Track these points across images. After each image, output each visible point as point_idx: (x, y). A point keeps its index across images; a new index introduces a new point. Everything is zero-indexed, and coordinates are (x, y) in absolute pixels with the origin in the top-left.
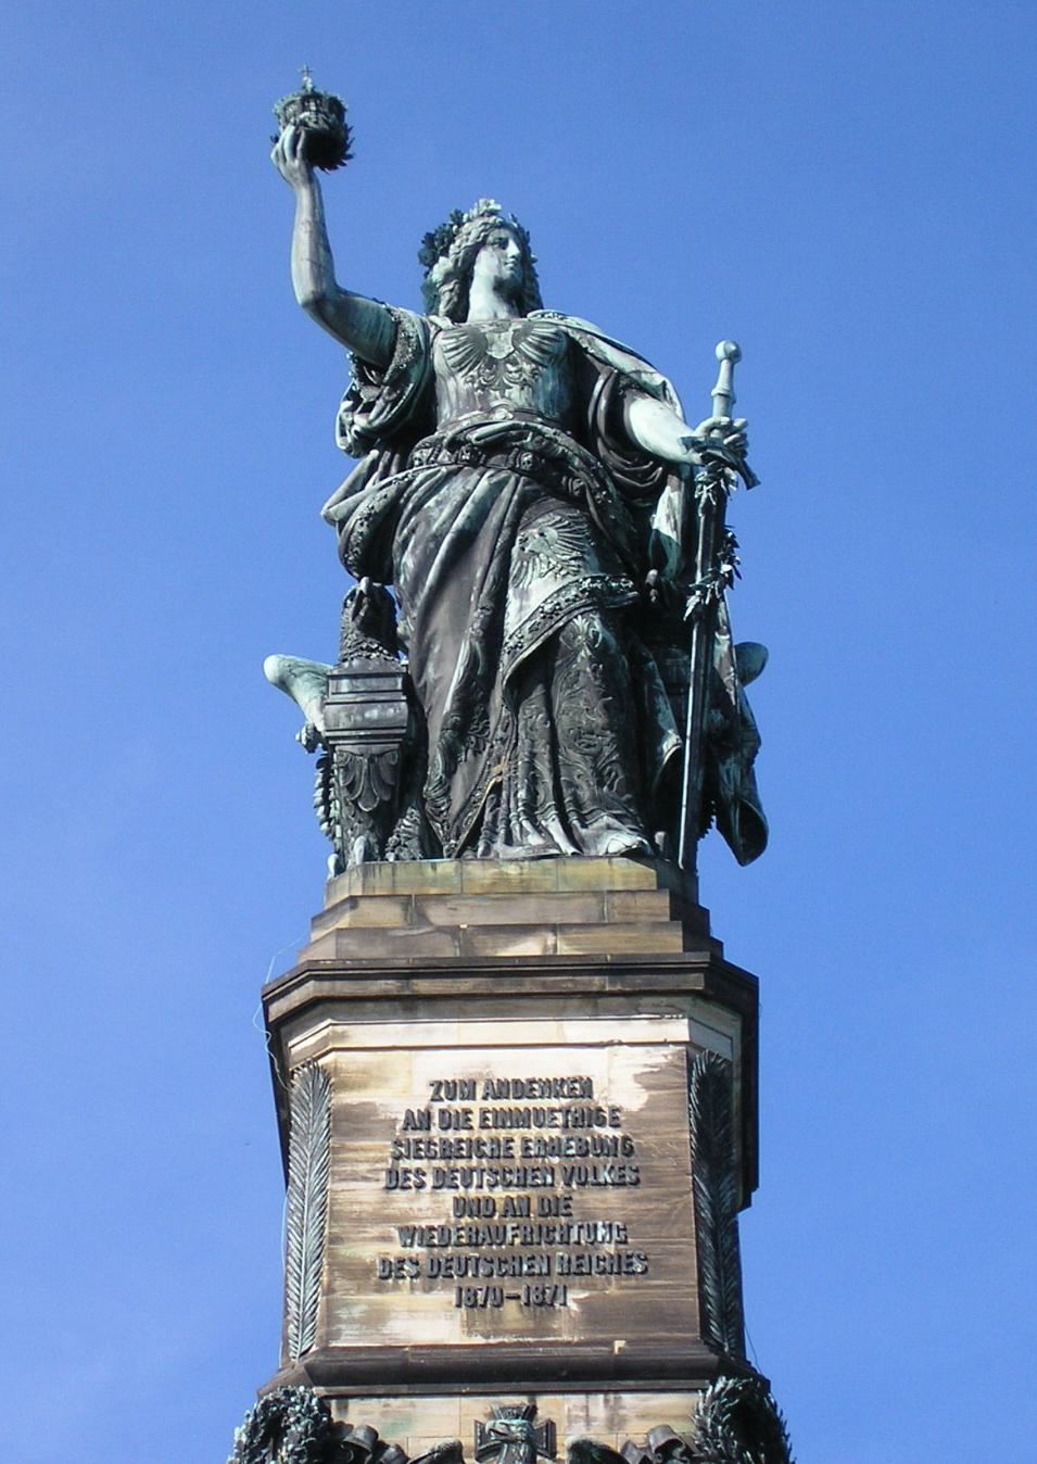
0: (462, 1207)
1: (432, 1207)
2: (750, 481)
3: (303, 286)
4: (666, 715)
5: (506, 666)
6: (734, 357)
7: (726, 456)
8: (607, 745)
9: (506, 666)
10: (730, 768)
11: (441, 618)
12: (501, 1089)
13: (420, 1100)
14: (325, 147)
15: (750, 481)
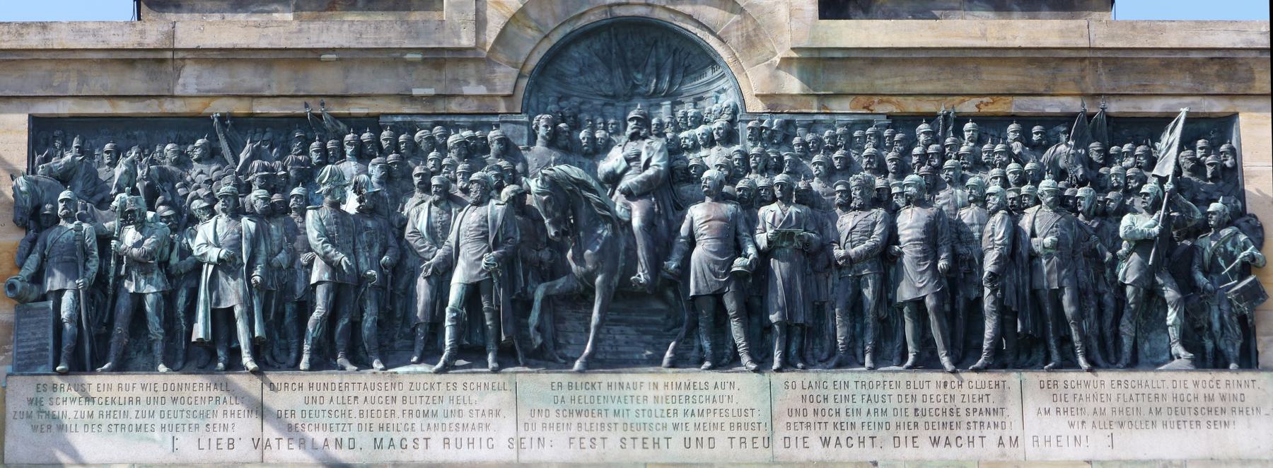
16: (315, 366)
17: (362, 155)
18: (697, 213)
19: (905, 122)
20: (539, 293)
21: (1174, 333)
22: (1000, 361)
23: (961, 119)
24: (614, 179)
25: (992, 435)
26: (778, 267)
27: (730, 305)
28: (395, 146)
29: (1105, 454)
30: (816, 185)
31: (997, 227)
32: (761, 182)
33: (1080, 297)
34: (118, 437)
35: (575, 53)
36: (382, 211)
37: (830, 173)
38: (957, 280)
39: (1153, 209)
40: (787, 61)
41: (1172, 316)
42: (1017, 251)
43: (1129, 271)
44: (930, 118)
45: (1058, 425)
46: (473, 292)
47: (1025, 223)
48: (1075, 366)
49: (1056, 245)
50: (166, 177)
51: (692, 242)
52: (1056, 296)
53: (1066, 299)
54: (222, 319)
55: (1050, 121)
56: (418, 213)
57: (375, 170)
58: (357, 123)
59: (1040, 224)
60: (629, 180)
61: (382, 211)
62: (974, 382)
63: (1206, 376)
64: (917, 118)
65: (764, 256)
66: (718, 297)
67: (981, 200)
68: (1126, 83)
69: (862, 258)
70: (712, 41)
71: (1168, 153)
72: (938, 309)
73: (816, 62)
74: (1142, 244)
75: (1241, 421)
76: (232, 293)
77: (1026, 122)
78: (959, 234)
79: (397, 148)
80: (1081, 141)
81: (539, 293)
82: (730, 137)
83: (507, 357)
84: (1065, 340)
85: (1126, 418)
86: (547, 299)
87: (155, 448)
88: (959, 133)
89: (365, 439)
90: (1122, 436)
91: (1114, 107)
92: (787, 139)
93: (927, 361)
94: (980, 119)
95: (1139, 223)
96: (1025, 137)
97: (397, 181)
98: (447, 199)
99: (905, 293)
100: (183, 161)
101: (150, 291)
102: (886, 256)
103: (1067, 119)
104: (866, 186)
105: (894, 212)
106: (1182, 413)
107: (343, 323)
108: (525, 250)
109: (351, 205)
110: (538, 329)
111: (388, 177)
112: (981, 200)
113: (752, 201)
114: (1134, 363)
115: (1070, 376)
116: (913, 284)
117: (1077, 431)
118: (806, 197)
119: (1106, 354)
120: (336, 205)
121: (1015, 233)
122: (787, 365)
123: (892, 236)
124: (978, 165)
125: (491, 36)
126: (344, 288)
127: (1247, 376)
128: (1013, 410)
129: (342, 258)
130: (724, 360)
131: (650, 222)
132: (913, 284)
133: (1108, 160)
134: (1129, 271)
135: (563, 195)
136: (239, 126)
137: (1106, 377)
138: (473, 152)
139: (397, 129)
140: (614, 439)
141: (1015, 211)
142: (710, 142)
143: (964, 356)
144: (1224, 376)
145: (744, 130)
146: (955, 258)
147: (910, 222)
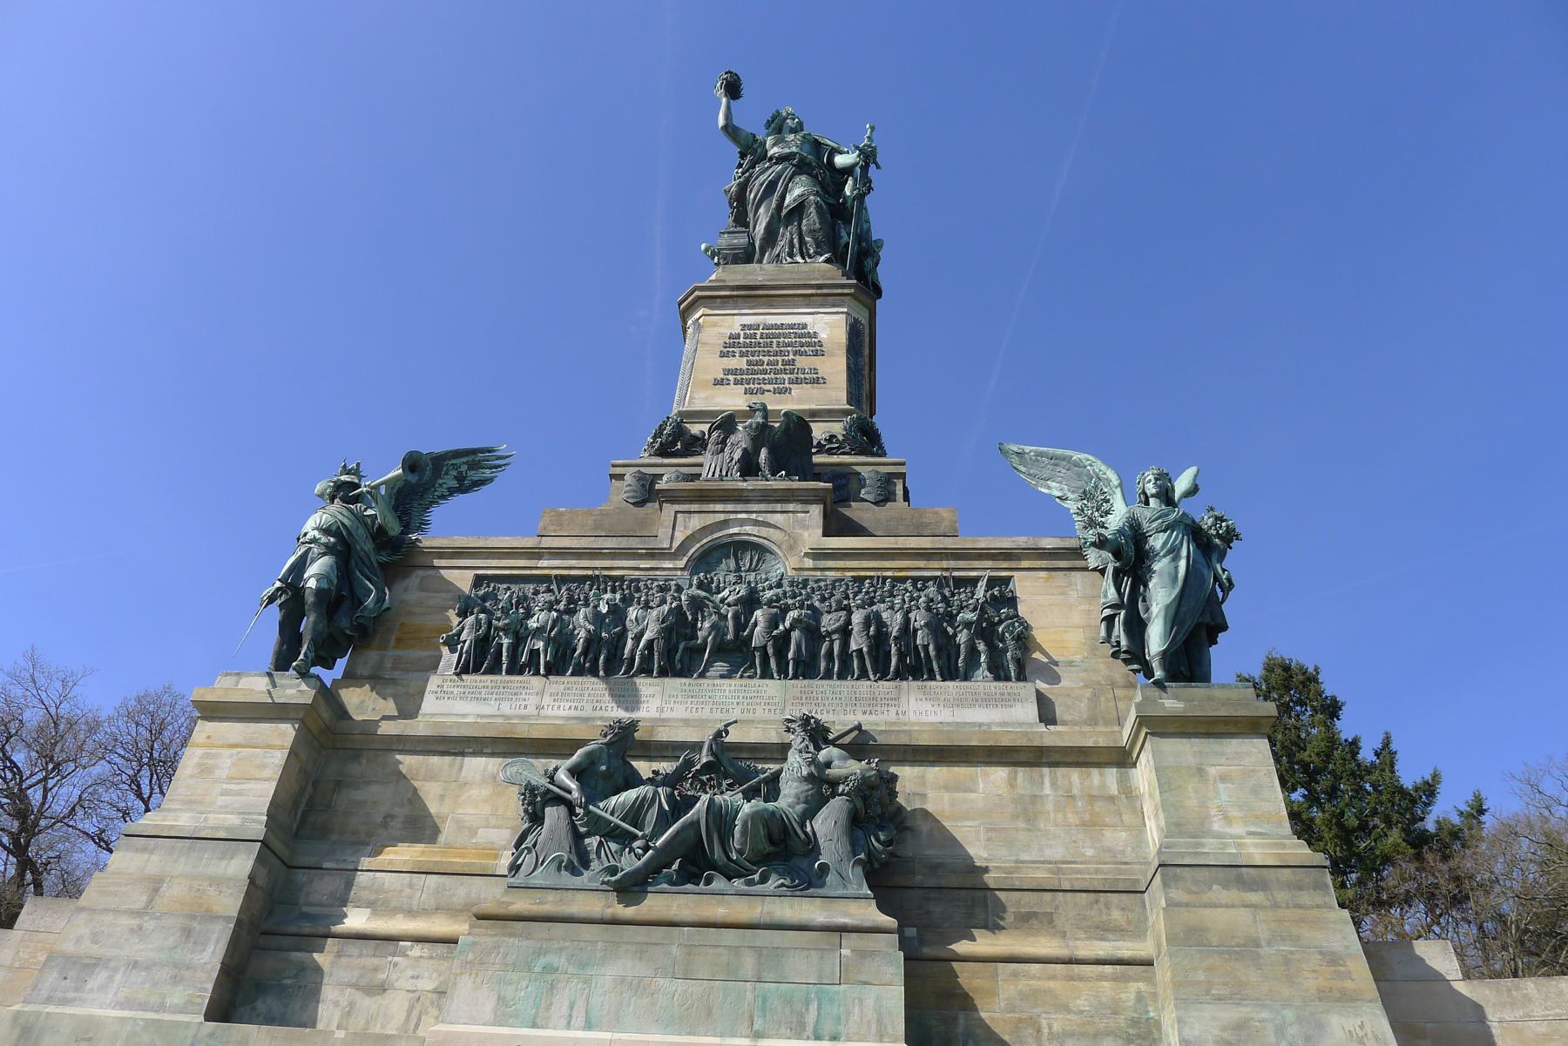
0: (749, 363)
1: (739, 363)
2: (878, 167)
3: (721, 121)
4: (843, 233)
5: (784, 212)
6: (873, 128)
7: (868, 156)
8: (820, 235)
9: (784, 212)
10: (869, 263)
11: (762, 210)
12: (767, 327)
13: (737, 330)
14: (733, 89)
15: (878, 167)
16: (573, 674)
17: (614, 591)
18: (758, 613)
19: (859, 580)
20: (681, 646)
21: (984, 665)
22: (900, 675)
23: (885, 579)
24: (723, 600)
25: (893, 710)
26: (795, 635)
27: (770, 651)
28: (629, 587)
29: (950, 720)
30: (817, 604)
31: (899, 617)
32: (790, 601)
33: (938, 649)
34: (474, 703)
35: (715, 554)
36: (618, 613)
37: (823, 599)
38: (879, 641)
39: (974, 610)
40: (806, 555)
41: (983, 658)
42: (907, 630)
43: (962, 638)
44: (871, 578)
45: (927, 706)
46: (650, 643)
47: (912, 615)
48: (934, 679)
49: (926, 625)
50: (525, 598)
51: (755, 624)
52: (926, 647)
53: (931, 648)
54: (534, 654)
55: (926, 580)
56: (633, 613)
57: (618, 596)
58: (614, 579)
59: (919, 618)
60: (730, 599)
61: (618, 613)
62: (885, 685)
63: (1001, 684)
64: (866, 578)
65: (788, 632)
66: (765, 647)
67: (892, 608)
68: (961, 564)
69: (834, 632)
70: (775, 548)
71: (980, 592)
72: (869, 652)
73: (818, 554)
74: (968, 625)
75: (1019, 705)
76: (540, 645)
77: (915, 580)
78: (881, 624)
79: (629, 591)
80: (940, 587)
81: (681, 646)
82: (779, 585)
83: (663, 673)
84: (931, 671)
85: (959, 703)
86: (686, 649)
87: (489, 708)
88: (884, 583)
89: (588, 707)
90: (958, 712)
91: (955, 574)
92: (805, 587)
93: (863, 675)
94: (895, 579)
95: (970, 616)
96: (914, 585)
97: (627, 601)
98: (647, 606)
99: (853, 646)
100: (536, 593)
101: (506, 641)
102: (845, 632)
103: (935, 578)
104: (839, 602)
105: (850, 613)
106: (988, 701)
107: (590, 656)
108: (678, 628)
109: (604, 609)
110: (681, 661)
111: (623, 599)
112: (892, 608)
113: (785, 610)
114: (966, 678)
115: (933, 683)
116: (857, 642)
117: (936, 708)
118: (811, 607)
119: (950, 674)
120: (596, 607)
121: (907, 620)
122: (795, 677)
123: (848, 622)
124: (892, 595)
125: (676, 545)
126: (592, 642)
127: (1021, 684)
128: (904, 699)
129: (592, 628)
130: (767, 674)
131: (736, 617)
132: (857, 642)
133: (953, 595)
134: (962, 638)
135: (697, 605)
136: (562, 580)
137: (950, 684)
138: (662, 589)
139: (631, 581)
140: (707, 709)
141: (909, 611)
142: (771, 588)
143: (882, 673)
144: (1009, 684)
145: (785, 582)
146: (878, 630)
147: (857, 618)
